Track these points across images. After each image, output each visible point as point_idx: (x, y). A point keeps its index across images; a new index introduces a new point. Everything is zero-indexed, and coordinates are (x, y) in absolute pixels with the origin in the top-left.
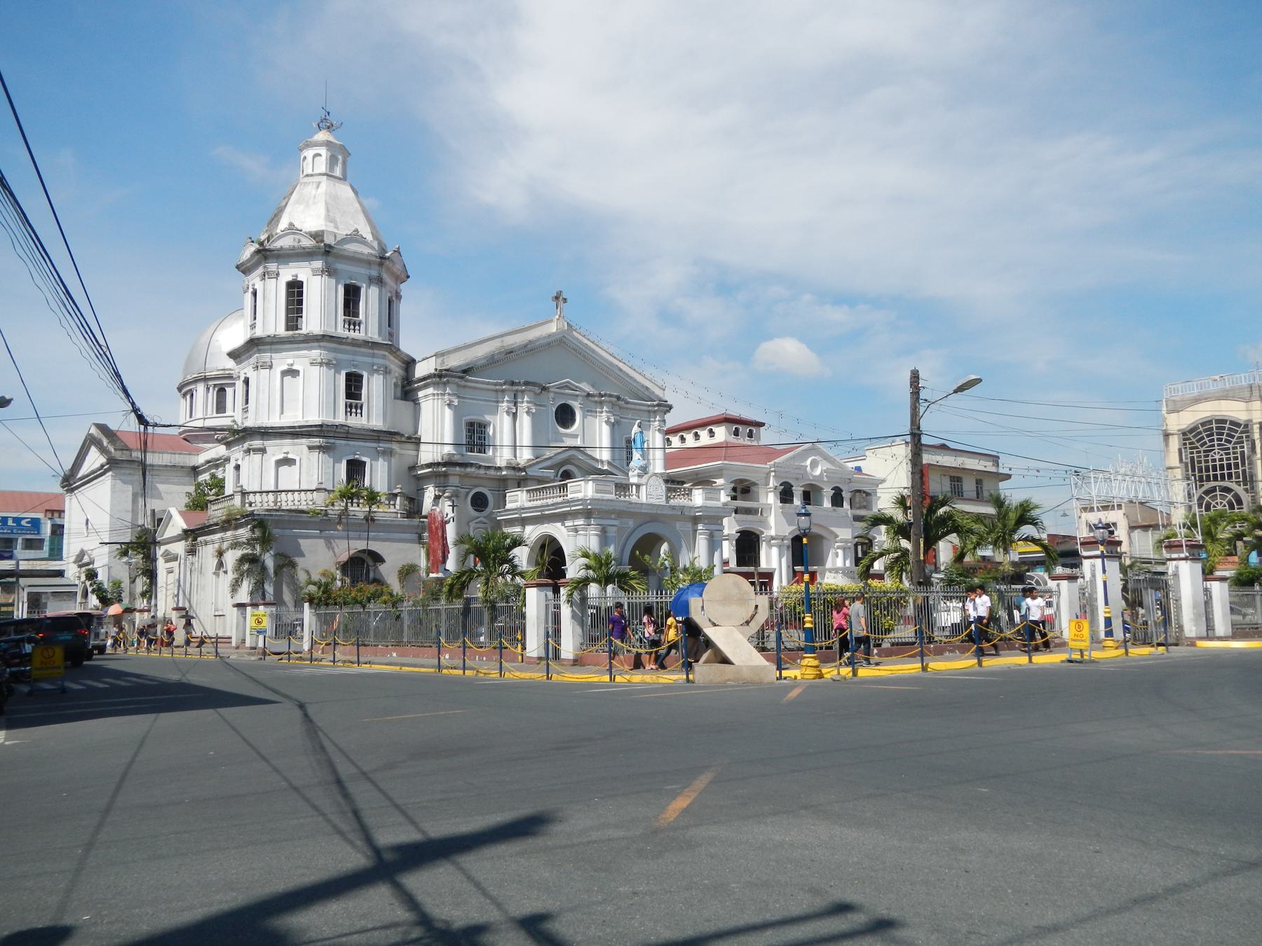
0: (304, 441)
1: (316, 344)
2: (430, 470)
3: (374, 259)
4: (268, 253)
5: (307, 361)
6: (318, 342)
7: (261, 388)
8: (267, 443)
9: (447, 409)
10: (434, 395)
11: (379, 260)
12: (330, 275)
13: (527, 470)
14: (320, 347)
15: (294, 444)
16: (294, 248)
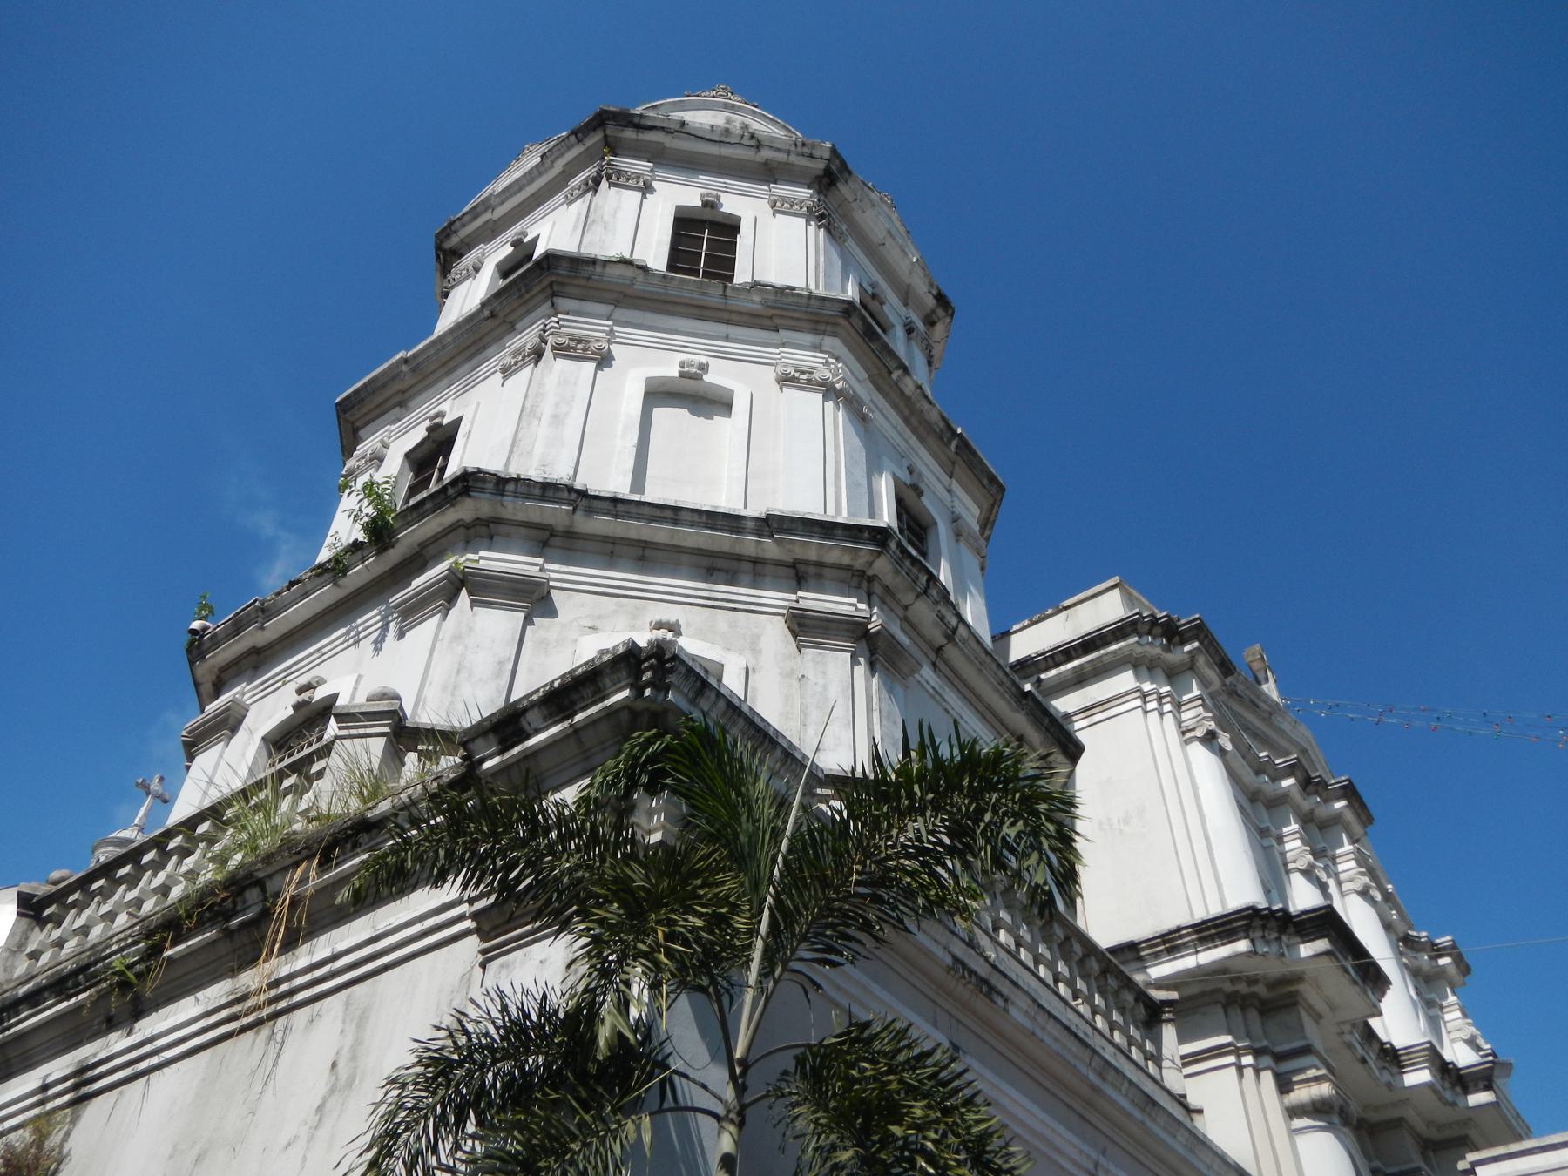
0: (778, 598)
1: (809, 338)
2: (1242, 946)
3: (920, 287)
4: (629, 134)
5: (769, 375)
6: (815, 331)
7: (547, 409)
8: (556, 572)
9: (1199, 752)
10: (1144, 696)
11: (931, 302)
12: (829, 231)
13: (1499, 1081)
14: (818, 348)
15: (711, 604)
16: (721, 137)
